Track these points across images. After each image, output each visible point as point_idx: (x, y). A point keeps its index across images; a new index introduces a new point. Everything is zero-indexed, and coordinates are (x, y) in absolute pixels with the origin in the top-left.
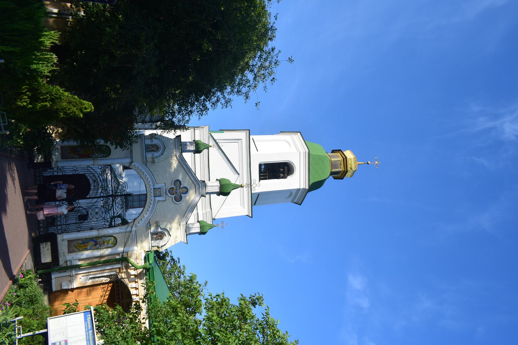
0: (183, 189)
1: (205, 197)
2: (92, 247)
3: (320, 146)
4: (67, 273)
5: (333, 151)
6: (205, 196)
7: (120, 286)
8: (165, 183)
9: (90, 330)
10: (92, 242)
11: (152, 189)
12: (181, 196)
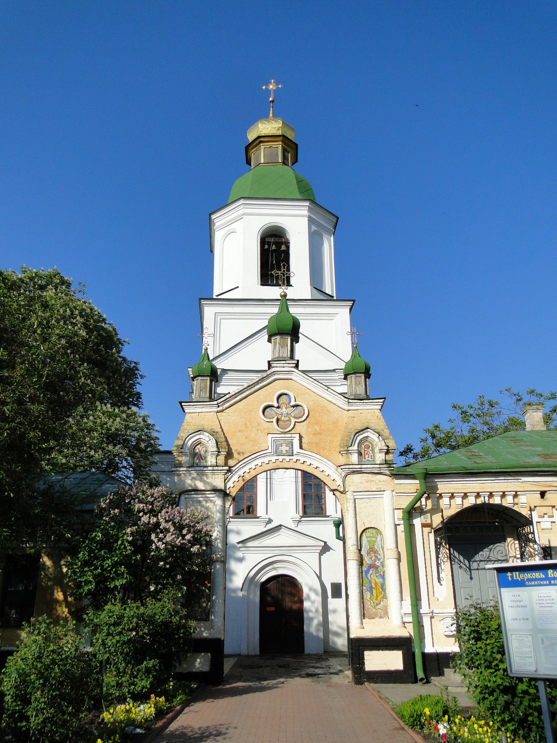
0: (281, 402)
1: (298, 361)
2: (380, 575)
3: (237, 182)
4: (426, 621)
5: (249, 162)
6: (296, 362)
7: (457, 525)
8: (268, 434)
9: (546, 575)
10: (371, 572)
11: (277, 458)
12: (293, 406)
